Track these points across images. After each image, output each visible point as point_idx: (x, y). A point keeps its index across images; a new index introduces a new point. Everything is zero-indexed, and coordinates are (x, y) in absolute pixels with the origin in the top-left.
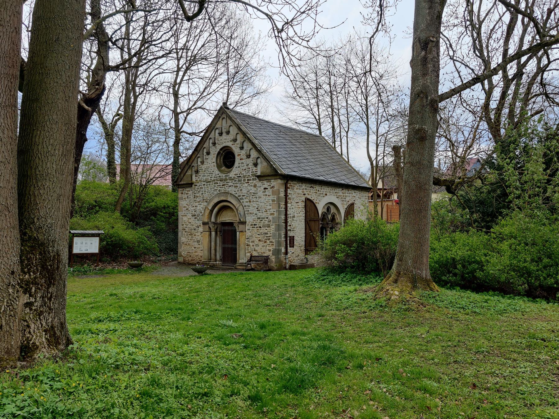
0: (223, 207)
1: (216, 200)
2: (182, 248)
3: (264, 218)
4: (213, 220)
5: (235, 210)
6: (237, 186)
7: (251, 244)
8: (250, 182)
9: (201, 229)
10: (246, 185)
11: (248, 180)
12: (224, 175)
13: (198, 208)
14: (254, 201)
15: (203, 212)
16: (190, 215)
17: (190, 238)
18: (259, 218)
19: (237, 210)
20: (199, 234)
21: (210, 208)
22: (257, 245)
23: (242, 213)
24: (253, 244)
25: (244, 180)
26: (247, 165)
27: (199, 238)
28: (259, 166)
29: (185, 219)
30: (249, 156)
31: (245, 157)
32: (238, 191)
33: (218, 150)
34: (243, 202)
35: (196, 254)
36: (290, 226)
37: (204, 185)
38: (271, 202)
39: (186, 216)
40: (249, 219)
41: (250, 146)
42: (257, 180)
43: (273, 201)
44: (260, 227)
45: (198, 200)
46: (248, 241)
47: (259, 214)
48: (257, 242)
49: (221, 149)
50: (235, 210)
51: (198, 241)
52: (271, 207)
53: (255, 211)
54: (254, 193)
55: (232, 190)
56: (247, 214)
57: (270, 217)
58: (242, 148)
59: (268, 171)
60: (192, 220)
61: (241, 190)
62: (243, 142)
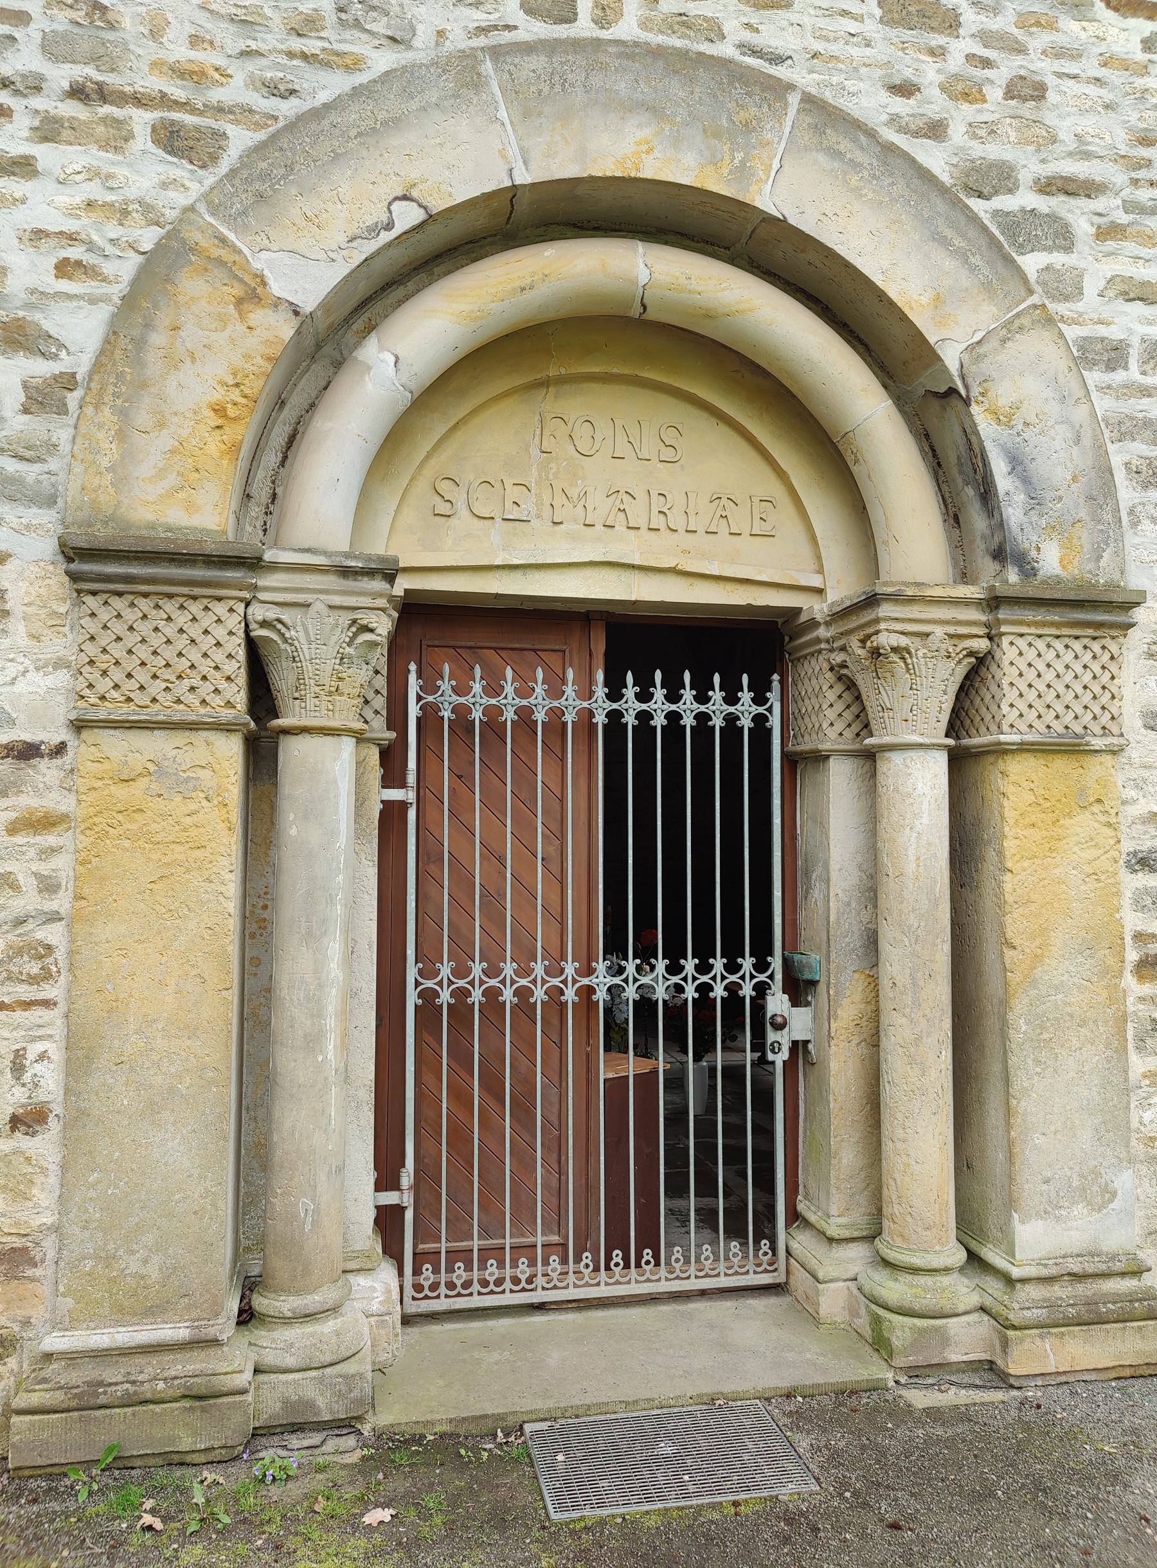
15: (80, 329)
19: (932, 403)
21: (307, 267)
32: (966, 92)
34: (1067, 287)
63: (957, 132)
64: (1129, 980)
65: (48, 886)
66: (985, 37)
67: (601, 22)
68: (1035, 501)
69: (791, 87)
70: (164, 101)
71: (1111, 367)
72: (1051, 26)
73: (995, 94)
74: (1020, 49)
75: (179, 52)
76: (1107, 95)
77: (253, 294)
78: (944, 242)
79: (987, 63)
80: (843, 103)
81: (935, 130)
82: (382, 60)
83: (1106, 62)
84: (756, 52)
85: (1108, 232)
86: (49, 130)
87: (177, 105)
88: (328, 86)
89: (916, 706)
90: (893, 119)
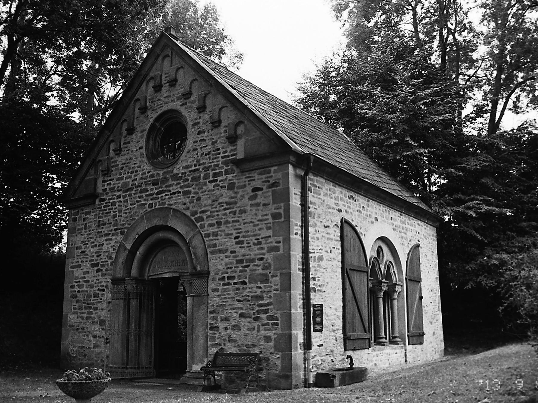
0: (158, 240)
3: (253, 260)
4: (134, 272)
5: (184, 248)
6: (189, 192)
7: (221, 325)
10: (211, 186)
11: (215, 175)
12: (161, 173)
13: (105, 248)
14: (227, 222)
15: (114, 256)
17: (85, 315)
18: (241, 261)
20: (104, 305)
21: (129, 246)
22: (236, 328)
23: (200, 252)
25: (206, 177)
26: (213, 143)
27: (103, 314)
28: (241, 143)
29: (78, 273)
30: (216, 124)
34: (202, 226)
35: (98, 350)
36: (314, 279)
37: (119, 197)
38: (271, 220)
39: (79, 266)
40: (217, 264)
41: (220, 100)
44: (244, 283)
45: (105, 230)
50: (184, 248)
53: (230, 243)
54: (227, 203)
55: (178, 202)
56: (212, 253)
57: (269, 257)
59: (264, 148)
61: (199, 199)
62: (206, 95)
63: (191, 208)
66: (195, 193)
68: (197, 260)
74: (198, 193)
75: (122, 223)
76: (208, 196)
77: (126, 249)
82: (137, 218)
85: (208, 217)
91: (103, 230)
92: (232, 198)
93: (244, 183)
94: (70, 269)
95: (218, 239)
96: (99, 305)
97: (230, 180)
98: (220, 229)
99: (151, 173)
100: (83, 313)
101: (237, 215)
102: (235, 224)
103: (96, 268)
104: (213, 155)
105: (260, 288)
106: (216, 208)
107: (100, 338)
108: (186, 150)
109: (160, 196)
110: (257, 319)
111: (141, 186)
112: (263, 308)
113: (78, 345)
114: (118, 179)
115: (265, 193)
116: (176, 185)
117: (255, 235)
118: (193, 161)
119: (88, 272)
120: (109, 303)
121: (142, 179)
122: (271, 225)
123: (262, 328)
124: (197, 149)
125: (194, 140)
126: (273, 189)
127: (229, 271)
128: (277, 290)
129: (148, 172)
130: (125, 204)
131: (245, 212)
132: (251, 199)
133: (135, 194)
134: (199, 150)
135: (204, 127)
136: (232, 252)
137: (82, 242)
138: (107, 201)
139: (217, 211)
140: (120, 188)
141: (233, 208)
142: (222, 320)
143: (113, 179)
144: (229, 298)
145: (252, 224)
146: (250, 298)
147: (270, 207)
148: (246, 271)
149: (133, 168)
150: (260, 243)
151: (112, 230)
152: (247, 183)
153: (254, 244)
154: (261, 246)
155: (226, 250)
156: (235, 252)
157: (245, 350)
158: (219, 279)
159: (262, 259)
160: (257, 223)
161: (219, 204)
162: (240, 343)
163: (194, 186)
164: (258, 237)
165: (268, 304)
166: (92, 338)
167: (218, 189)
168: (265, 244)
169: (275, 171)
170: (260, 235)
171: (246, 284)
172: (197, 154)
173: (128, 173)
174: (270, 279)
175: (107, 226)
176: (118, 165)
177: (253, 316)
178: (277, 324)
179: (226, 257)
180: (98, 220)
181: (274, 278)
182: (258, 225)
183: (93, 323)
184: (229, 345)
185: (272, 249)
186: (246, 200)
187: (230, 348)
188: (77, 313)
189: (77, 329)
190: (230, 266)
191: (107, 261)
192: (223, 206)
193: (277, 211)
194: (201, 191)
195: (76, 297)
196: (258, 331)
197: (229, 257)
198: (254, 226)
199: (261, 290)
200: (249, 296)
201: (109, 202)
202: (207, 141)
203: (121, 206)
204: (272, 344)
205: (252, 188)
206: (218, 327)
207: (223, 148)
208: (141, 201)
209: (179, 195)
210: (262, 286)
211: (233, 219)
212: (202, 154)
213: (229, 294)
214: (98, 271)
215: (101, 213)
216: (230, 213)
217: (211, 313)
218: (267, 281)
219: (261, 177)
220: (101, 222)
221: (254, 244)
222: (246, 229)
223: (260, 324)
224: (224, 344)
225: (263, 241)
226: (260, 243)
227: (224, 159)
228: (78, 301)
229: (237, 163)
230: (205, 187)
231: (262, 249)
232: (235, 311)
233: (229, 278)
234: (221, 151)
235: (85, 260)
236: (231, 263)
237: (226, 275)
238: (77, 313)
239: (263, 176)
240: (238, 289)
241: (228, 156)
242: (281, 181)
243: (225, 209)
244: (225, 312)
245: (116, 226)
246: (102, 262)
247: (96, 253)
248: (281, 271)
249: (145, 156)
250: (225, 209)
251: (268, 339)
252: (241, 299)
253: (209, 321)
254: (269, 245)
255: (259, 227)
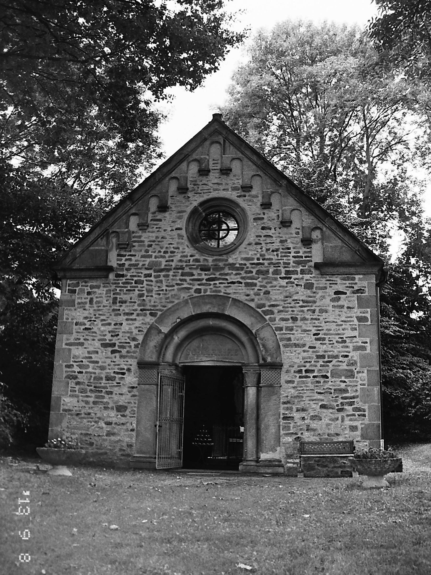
1: (185, 314)
2: (64, 424)
3: (336, 357)
5: (244, 339)
6: (255, 285)
8: (294, 276)
9: (131, 379)
10: (283, 282)
11: (287, 272)
12: (210, 259)
13: (125, 327)
14: (304, 319)
15: (140, 338)
16: (97, 344)
17: (91, 400)
18: (323, 357)
19: (253, 337)
20: (125, 390)
21: (165, 330)
24: (303, 414)
25: (276, 272)
27: (122, 401)
29: (77, 351)
30: (286, 223)
31: (277, 223)
33: (195, 204)
38: (356, 322)
39: (82, 344)
40: (291, 358)
42: (315, 273)
43: (360, 319)
45: (125, 308)
46: (287, 409)
47: (321, 349)
48: (314, 408)
49: (202, 204)
51: (120, 409)
52: (356, 333)
53: (309, 340)
55: (239, 292)
56: (286, 346)
57: (355, 355)
58: (266, 205)
60: (103, 356)
63: (256, 300)
64: (281, 420)
65: (135, 403)
66: (261, 286)
67: (204, 293)
68: (266, 351)
69: (230, 297)
70: (151, 310)
71: (280, 331)
72: (271, 283)
73: (262, 294)
75: (152, 304)
77: (160, 332)
78: (253, 316)
79: (261, 290)
80: (239, 298)
81: (253, 300)
82: (176, 301)
83: (280, 287)
84: (226, 293)
86: (138, 315)
87: (153, 310)
88: (170, 305)
89: (250, 379)
90: (246, 300)
91: (121, 309)
92: (310, 297)
93: (325, 285)
94: (64, 346)
95: (293, 334)
96: (116, 389)
97: (307, 280)
98: (295, 324)
99: (194, 258)
100: (87, 396)
101: (317, 313)
102: (314, 321)
103: (110, 349)
104: (281, 252)
105: (345, 382)
106: (290, 304)
107: (119, 425)
108: (246, 242)
109: (212, 283)
110: (339, 410)
111: (183, 269)
112: (348, 400)
113: (80, 432)
114: (142, 257)
115: (349, 297)
116: (236, 274)
117: (339, 334)
118: (256, 254)
119: (97, 352)
120: (133, 387)
121: (181, 261)
122: (357, 326)
123: (346, 419)
124: (261, 244)
125: (257, 234)
126: (358, 295)
127: (308, 365)
128: (364, 385)
129: (191, 256)
130: (159, 284)
131: (326, 312)
132: (333, 300)
133: (173, 276)
134: (263, 245)
135: (270, 224)
136: (310, 347)
137: (86, 318)
138: (128, 277)
139: (292, 307)
140: (146, 266)
141: (312, 306)
142: (298, 410)
143: (135, 255)
144: (306, 390)
145: (335, 324)
146: (332, 391)
147: (355, 310)
148: (328, 366)
149: (167, 248)
150: (345, 342)
151: (136, 310)
152: (328, 285)
153: (337, 342)
154: (345, 344)
155: (304, 345)
156: (315, 348)
157: (327, 439)
158: (294, 372)
159: (347, 356)
160: (342, 323)
161: (293, 300)
162: (320, 432)
163: (259, 279)
164: (342, 336)
165: (354, 397)
166: (104, 425)
167: (293, 286)
168: (350, 343)
169: (360, 279)
170: (344, 334)
171: (327, 377)
172: (261, 249)
173: (160, 252)
174: (356, 375)
175: (128, 304)
176: (143, 242)
177: (337, 408)
178: (364, 415)
179: (304, 351)
180: (112, 296)
181: (360, 375)
182: (342, 325)
183: (106, 408)
184: (306, 434)
185: (357, 348)
186: (327, 301)
187: (307, 437)
188: (77, 396)
189: (78, 415)
190: (308, 360)
191: (129, 343)
192: (298, 303)
193: (363, 315)
194: (270, 285)
195: (76, 377)
196: (343, 421)
197: (308, 351)
198: (337, 325)
199: (345, 384)
200: (331, 389)
201: (133, 280)
202: (274, 239)
203: (152, 286)
204: (359, 433)
205: (334, 291)
206: (293, 417)
207: (294, 248)
208: (182, 284)
209: (240, 285)
210: (346, 380)
211: (312, 317)
212: (268, 250)
213: (307, 386)
214: (113, 352)
215: (118, 289)
216: (308, 310)
217: (284, 403)
218: (352, 376)
219: (344, 282)
220: (118, 299)
221: (337, 342)
222: (328, 327)
223: (345, 415)
224: (302, 433)
225: (348, 340)
226: (345, 342)
227: (297, 259)
228: (78, 383)
229: (317, 266)
230: (275, 283)
231: (347, 347)
232: (314, 402)
233: (306, 371)
234: (292, 250)
235: (90, 338)
236: (310, 358)
237: (304, 369)
238: (77, 396)
239: (347, 282)
240: (318, 382)
241: (302, 257)
242: (366, 289)
243: (301, 307)
244: (303, 403)
245: (144, 305)
246: (120, 343)
247: (109, 332)
248: (369, 369)
249: (185, 237)
250: (301, 307)
251: (353, 428)
252: (322, 391)
253: (282, 411)
254: (355, 344)
255: (343, 327)
